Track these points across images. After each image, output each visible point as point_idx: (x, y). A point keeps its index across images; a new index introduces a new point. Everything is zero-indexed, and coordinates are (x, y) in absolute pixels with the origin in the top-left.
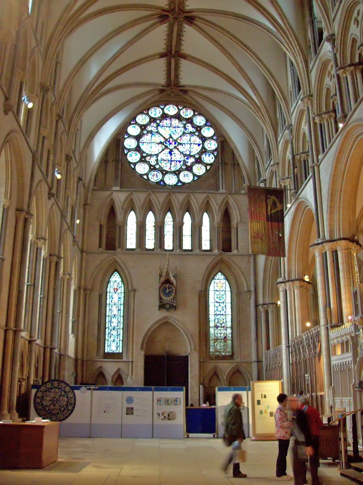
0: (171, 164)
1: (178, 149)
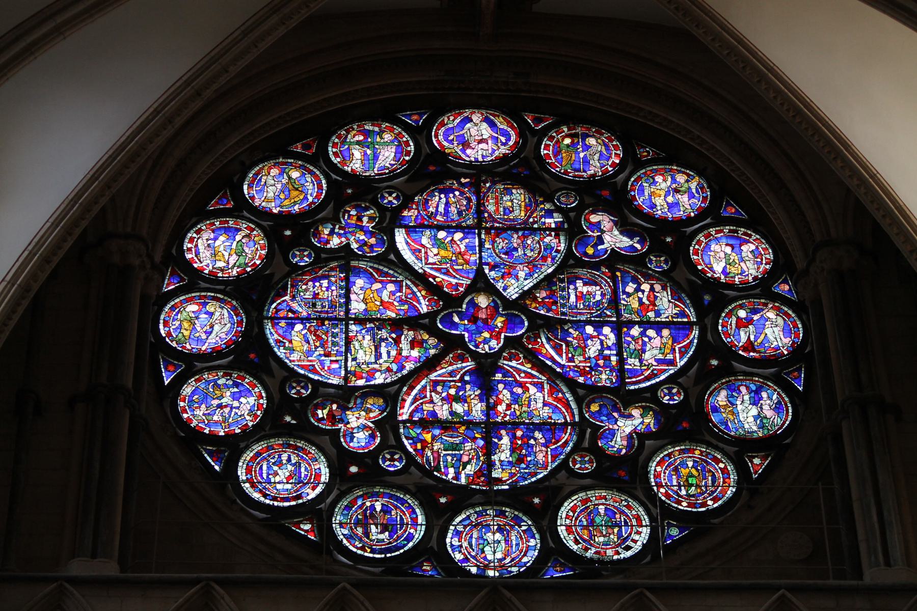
0: (490, 449)
1: (533, 357)
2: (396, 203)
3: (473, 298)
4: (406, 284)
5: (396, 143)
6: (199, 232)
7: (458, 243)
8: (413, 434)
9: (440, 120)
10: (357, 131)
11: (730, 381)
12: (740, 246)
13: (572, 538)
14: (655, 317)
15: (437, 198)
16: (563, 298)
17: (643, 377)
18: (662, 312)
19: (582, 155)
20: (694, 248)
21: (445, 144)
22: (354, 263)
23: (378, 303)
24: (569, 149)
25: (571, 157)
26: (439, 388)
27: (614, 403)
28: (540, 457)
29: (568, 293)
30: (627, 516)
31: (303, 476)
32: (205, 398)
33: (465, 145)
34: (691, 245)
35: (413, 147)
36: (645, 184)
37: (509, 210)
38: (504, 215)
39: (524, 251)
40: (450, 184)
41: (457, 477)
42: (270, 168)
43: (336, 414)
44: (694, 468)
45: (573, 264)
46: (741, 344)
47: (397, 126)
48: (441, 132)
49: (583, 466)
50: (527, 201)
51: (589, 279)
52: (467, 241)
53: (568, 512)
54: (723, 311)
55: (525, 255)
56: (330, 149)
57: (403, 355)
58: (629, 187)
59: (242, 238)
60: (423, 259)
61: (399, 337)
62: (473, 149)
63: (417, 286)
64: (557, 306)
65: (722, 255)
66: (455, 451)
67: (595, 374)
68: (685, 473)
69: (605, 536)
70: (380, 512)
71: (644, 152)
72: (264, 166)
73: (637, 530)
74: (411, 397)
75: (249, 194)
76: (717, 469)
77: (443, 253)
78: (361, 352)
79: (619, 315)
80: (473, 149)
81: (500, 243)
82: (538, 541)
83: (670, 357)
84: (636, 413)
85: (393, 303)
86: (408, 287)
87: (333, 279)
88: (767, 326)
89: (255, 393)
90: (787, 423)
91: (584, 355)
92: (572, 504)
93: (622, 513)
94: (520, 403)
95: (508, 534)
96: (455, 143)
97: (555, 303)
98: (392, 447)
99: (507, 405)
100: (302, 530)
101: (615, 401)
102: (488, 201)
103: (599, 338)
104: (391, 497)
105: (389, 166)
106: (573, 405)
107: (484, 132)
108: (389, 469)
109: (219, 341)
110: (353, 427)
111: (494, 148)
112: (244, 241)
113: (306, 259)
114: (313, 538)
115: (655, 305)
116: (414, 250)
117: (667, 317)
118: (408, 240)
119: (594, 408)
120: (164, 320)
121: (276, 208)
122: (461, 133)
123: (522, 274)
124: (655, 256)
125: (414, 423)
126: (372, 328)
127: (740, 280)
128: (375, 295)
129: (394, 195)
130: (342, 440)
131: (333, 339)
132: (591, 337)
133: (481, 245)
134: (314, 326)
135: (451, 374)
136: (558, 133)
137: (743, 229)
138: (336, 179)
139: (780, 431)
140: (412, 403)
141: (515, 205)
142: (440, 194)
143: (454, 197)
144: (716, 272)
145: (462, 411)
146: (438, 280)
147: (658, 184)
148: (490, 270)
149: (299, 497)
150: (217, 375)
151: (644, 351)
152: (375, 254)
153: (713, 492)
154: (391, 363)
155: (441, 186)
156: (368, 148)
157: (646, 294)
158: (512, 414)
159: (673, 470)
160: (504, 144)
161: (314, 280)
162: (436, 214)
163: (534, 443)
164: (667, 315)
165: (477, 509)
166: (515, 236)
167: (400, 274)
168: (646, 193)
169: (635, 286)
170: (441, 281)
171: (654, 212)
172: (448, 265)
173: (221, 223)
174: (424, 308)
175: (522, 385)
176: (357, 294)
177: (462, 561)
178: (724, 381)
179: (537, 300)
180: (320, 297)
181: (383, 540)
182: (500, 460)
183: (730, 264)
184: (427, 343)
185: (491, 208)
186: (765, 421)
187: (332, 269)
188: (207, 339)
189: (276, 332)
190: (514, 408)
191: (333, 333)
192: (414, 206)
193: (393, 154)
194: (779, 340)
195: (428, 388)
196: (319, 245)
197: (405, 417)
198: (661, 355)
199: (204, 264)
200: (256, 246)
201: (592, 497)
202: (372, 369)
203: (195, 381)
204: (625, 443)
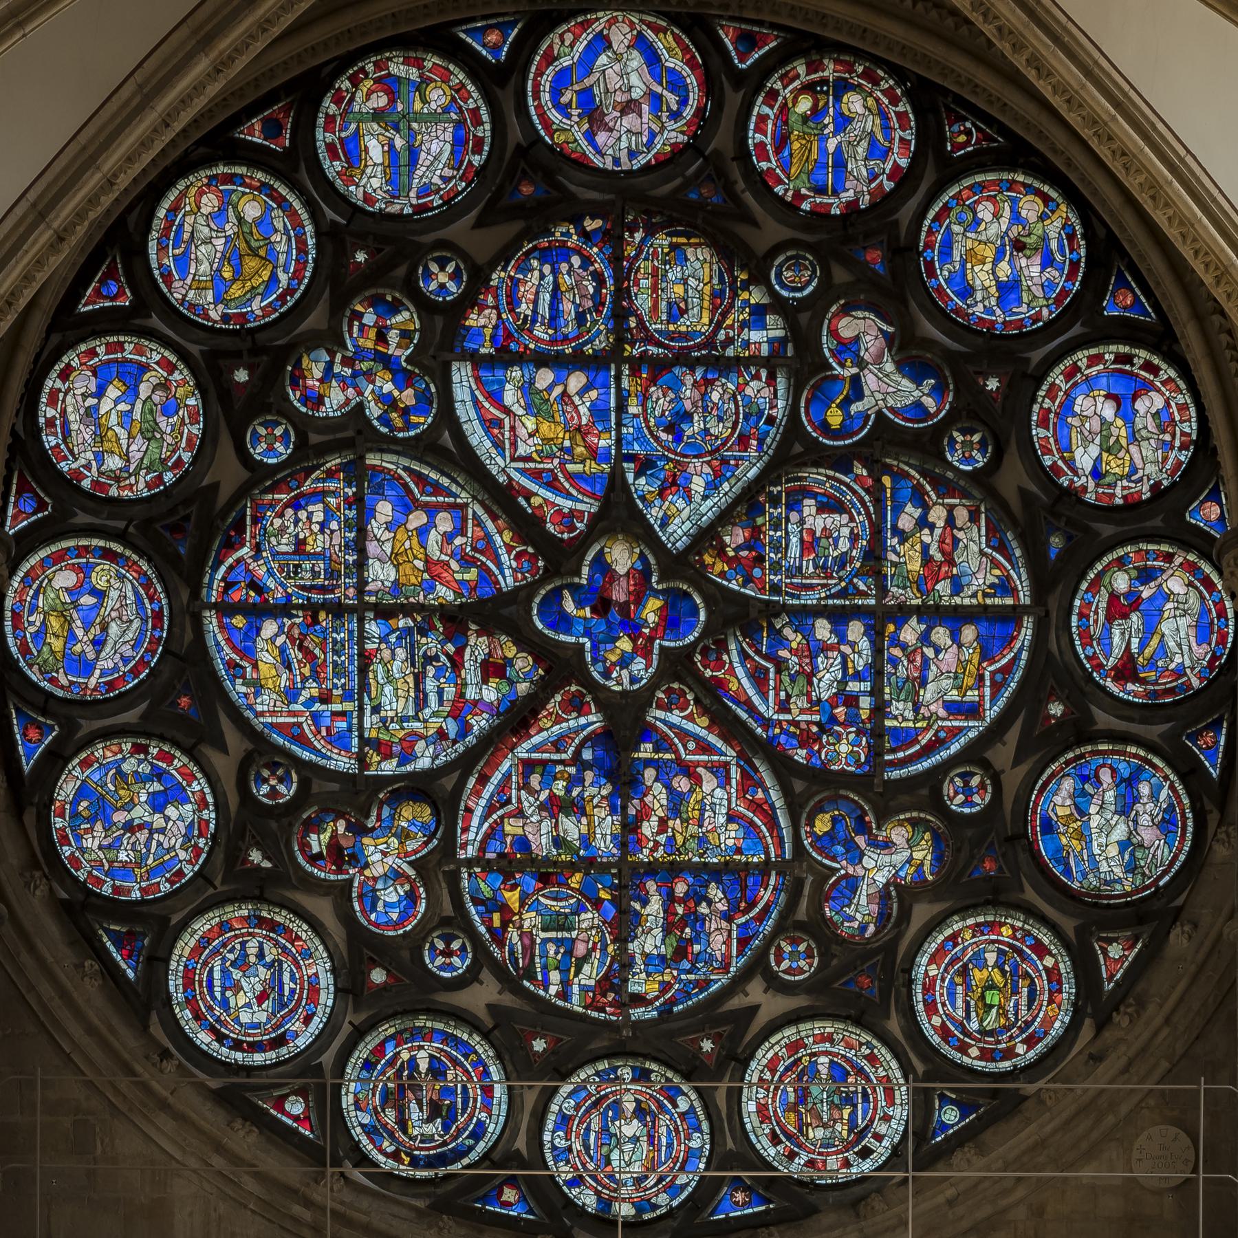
2: (454, 289)
3: (602, 549)
4: (474, 512)
5: (455, 117)
6: (65, 375)
7: (576, 400)
8: (486, 891)
9: (544, 47)
10: (376, 81)
11: (1082, 756)
12: (1134, 399)
13: (767, 1131)
14: (951, 596)
15: (536, 273)
16: (776, 547)
17: (918, 747)
18: (964, 580)
19: (832, 145)
20: (1041, 407)
21: (555, 116)
22: (372, 460)
23: (420, 564)
24: (807, 130)
25: (810, 151)
26: (535, 780)
27: (859, 812)
28: (718, 940)
29: (787, 533)
30: (868, 1079)
31: (287, 993)
32: (101, 811)
33: (594, 115)
34: (1033, 400)
35: (487, 126)
36: (956, 228)
37: (679, 308)
38: (668, 323)
39: (705, 422)
40: (562, 234)
41: (564, 995)
42: (201, 193)
43: (344, 843)
44: (998, 967)
45: (800, 455)
46: (1111, 662)
47: (457, 65)
48: (546, 81)
49: (794, 965)
50: (715, 281)
51: (830, 496)
52: (593, 394)
53: (762, 1072)
54: (1083, 576)
55: (706, 431)
56: (320, 134)
57: (468, 697)
58: (923, 236)
59: (153, 392)
60: (507, 442)
61: (460, 651)
62: (611, 130)
63: (494, 518)
64: (763, 569)
65: (1095, 424)
66: (562, 930)
67: (828, 743)
68: (981, 980)
69: (825, 1126)
70: (427, 1075)
71: (960, 133)
72: (187, 187)
73: (885, 1114)
74: (483, 802)
75: (161, 266)
76: (1039, 971)
77: (545, 427)
78: (388, 689)
79: (883, 591)
80: (611, 130)
81: (658, 399)
82: (706, 1137)
83: (972, 695)
84: (899, 835)
85: (447, 564)
86: (478, 522)
87: (332, 501)
88: (1166, 615)
89: (193, 793)
90: (1182, 858)
91: (809, 695)
92: (769, 1055)
93: (860, 1072)
94: (684, 816)
95: (653, 1122)
96: (575, 112)
97: (760, 560)
98: (445, 922)
99: (660, 818)
100: (289, 1115)
101: (861, 808)
102: (637, 283)
103: (839, 651)
104: (448, 1038)
105: (440, 182)
106: (783, 821)
107: (634, 79)
108: (443, 974)
109: (121, 664)
110: (376, 875)
111: (654, 126)
112: (156, 398)
113: (279, 447)
114: (307, 1133)
115: (951, 562)
116: (490, 421)
117: (974, 595)
118: (477, 393)
119: (822, 825)
120: (13, 611)
121: (216, 303)
122: (587, 82)
123: (698, 485)
124: (964, 432)
125: (488, 866)
126: (408, 631)
127: (1125, 492)
128: (415, 541)
129: (450, 268)
130: (357, 906)
131: (335, 658)
132: (825, 648)
133: (621, 408)
134: (299, 625)
135: (558, 744)
136: (787, 79)
137: (1143, 354)
138: (333, 222)
139: (1167, 878)
140: (485, 818)
141: (690, 291)
142: (542, 265)
143: (569, 273)
144: (1080, 472)
145: (576, 836)
146: (536, 501)
147: (983, 226)
148: (638, 475)
149: (280, 1041)
150: (121, 751)
151: (923, 683)
152: (412, 433)
153: (1028, 1024)
154: (445, 718)
155: (544, 242)
156: (398, 130)
157: (938, 532)
158: (672, 840)
159: (958, 973)
160: (675, 116)
161: (296, 504)
162: (534, 321)
163: (706, 911)
164: (975, 588)
165: (601, 1067)
166: (689, 380)
167: (463, 488)
168: (956, 256)
169: (917, 513)
170: (541, 506)
171: (969, 306)
172: (556, 461)
173: (111, 348)
174: (508, 581)
175: (688, 770)
176: (378, 540)
177: (572, 1183)
178: (1070, 755)
179: (725, 553)
180: (308, 548)
181: (431, 1138)
182: (643, 953)
183: (1108, 450)
184: (512, 666)
185: (643, 302)
186: (1139, 854)
187: (331, 474)
188: (97, 658)
189: (228, 641)
190: (673, 829)
191: (335, 641)
192: (490, 299)
193: (448, 147)
194: (1185, 648)
195: (514, 778)
196: (304, 410)
197: (471, 851)
198: (955, 692)
199: (83, 462)
200: (181, 413)
201: (807, 1037)
202: (408, 734)
203: (82, 764)
204: (875, 908)
